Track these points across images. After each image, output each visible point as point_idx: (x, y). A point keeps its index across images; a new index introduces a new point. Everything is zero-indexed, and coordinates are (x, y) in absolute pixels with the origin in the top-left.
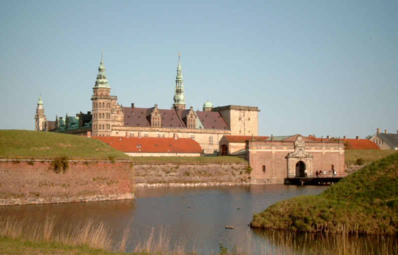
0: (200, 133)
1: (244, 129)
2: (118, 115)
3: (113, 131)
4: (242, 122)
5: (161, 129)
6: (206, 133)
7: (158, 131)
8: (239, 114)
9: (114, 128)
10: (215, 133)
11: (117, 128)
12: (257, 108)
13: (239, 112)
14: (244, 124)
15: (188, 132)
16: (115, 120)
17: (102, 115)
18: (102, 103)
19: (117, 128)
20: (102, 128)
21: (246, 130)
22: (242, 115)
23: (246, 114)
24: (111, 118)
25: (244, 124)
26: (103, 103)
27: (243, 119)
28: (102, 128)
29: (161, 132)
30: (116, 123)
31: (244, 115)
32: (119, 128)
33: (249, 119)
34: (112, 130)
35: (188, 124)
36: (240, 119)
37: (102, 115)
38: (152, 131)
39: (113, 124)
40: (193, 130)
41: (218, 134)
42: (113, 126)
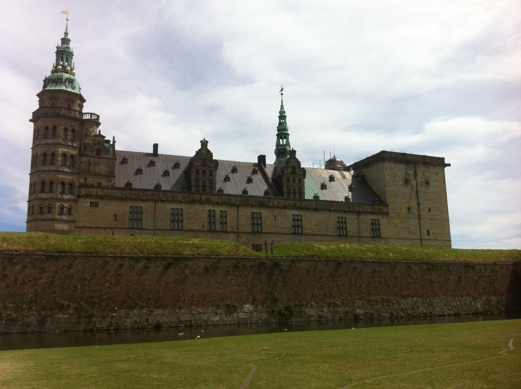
0: (316, 209)
1: (419, 204)
2: (97, 160)
3: (82, 200)
4: (412, 188)
5: (216, 199)
6: (330, 211)
7: (208, 202)
8: (403, 171)
9: (83, 191)
10: (352, 212)
11: (93, 191)
12: (443, 159)
13: (403, 166)
14: (417, 192)
15: (285, 208)
16: (89, 172)
17: (49, 158)
18: (51, 127)
19: (93, 191)
20: (47, 189)
21: (421, 206)
22: (411, 172)
23: (419, 172)
24: (76, 166)
25: (417, 192)
26: (55, 128)
27: (414, 183)
28: (47, 189)
29: (218, 204)
30: (90, 180)
31: (416, 174)
32: (100, 192)
33: (427, 183)
34: (79, 197)
35: (285, 189)
36: (407, 181)
37: (49, 158)
38: (193, 202)
39: (82, 181)
40: (298, 204)
41: (359, 213)
42: (81, 186)
